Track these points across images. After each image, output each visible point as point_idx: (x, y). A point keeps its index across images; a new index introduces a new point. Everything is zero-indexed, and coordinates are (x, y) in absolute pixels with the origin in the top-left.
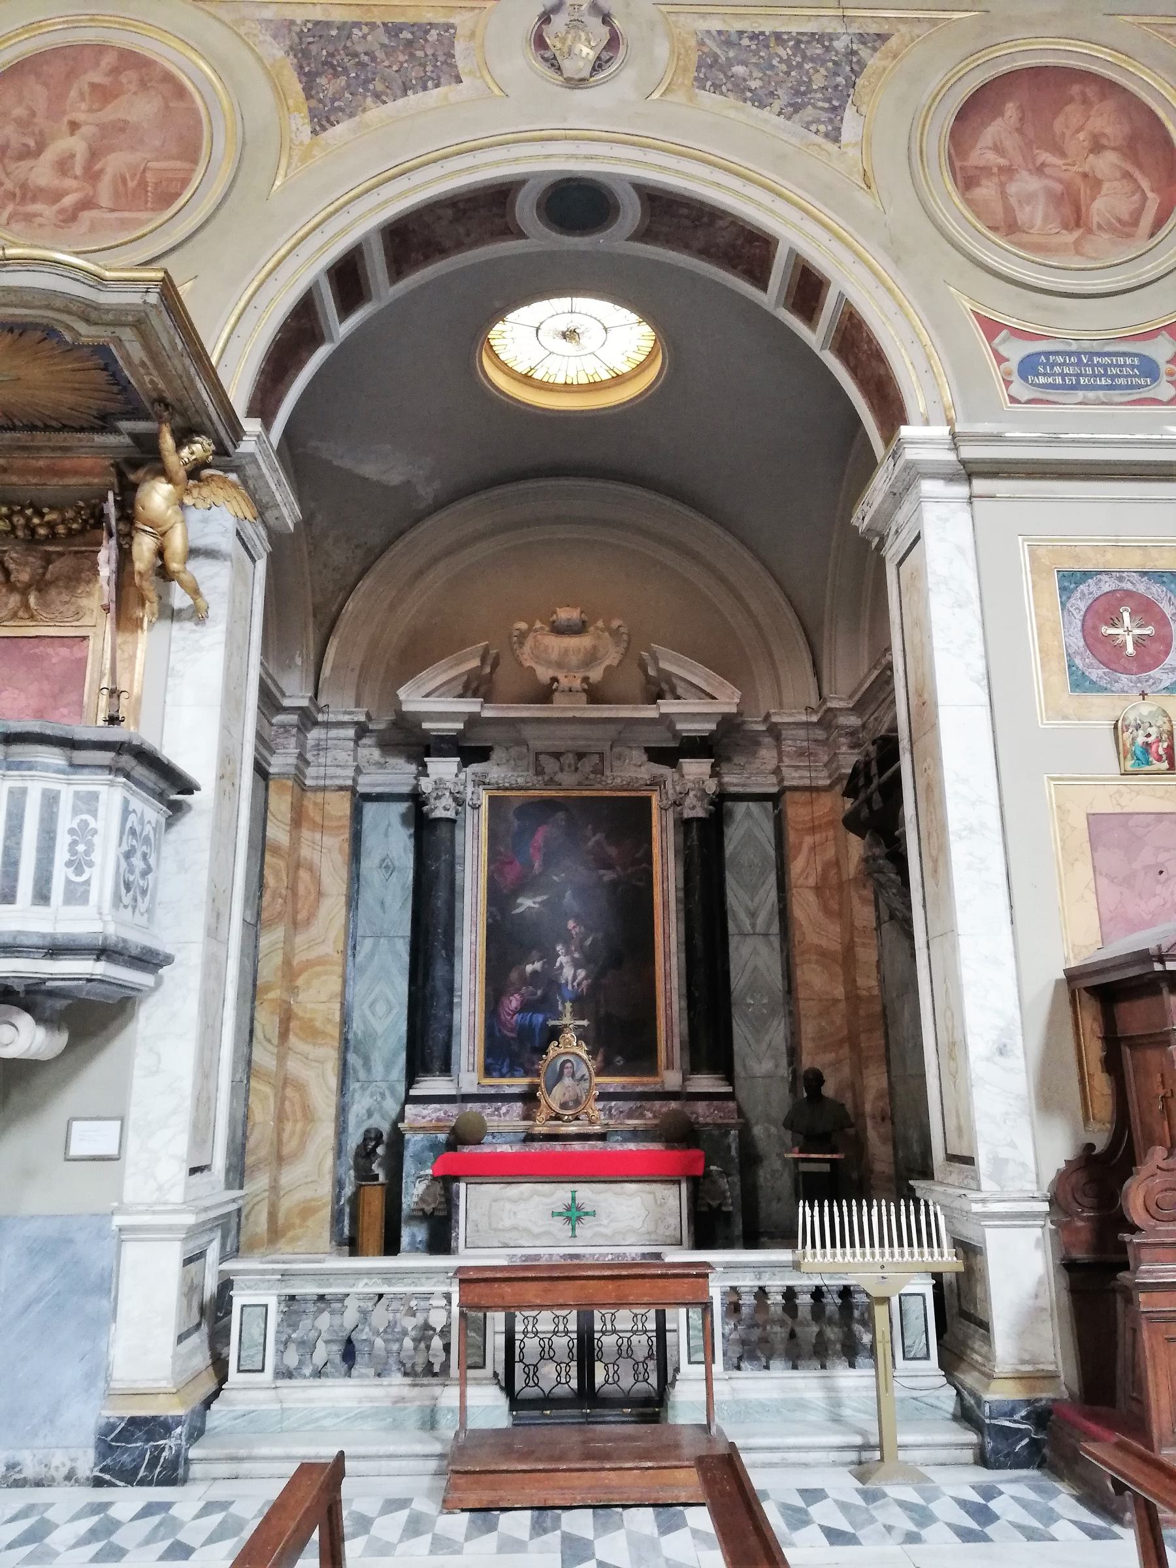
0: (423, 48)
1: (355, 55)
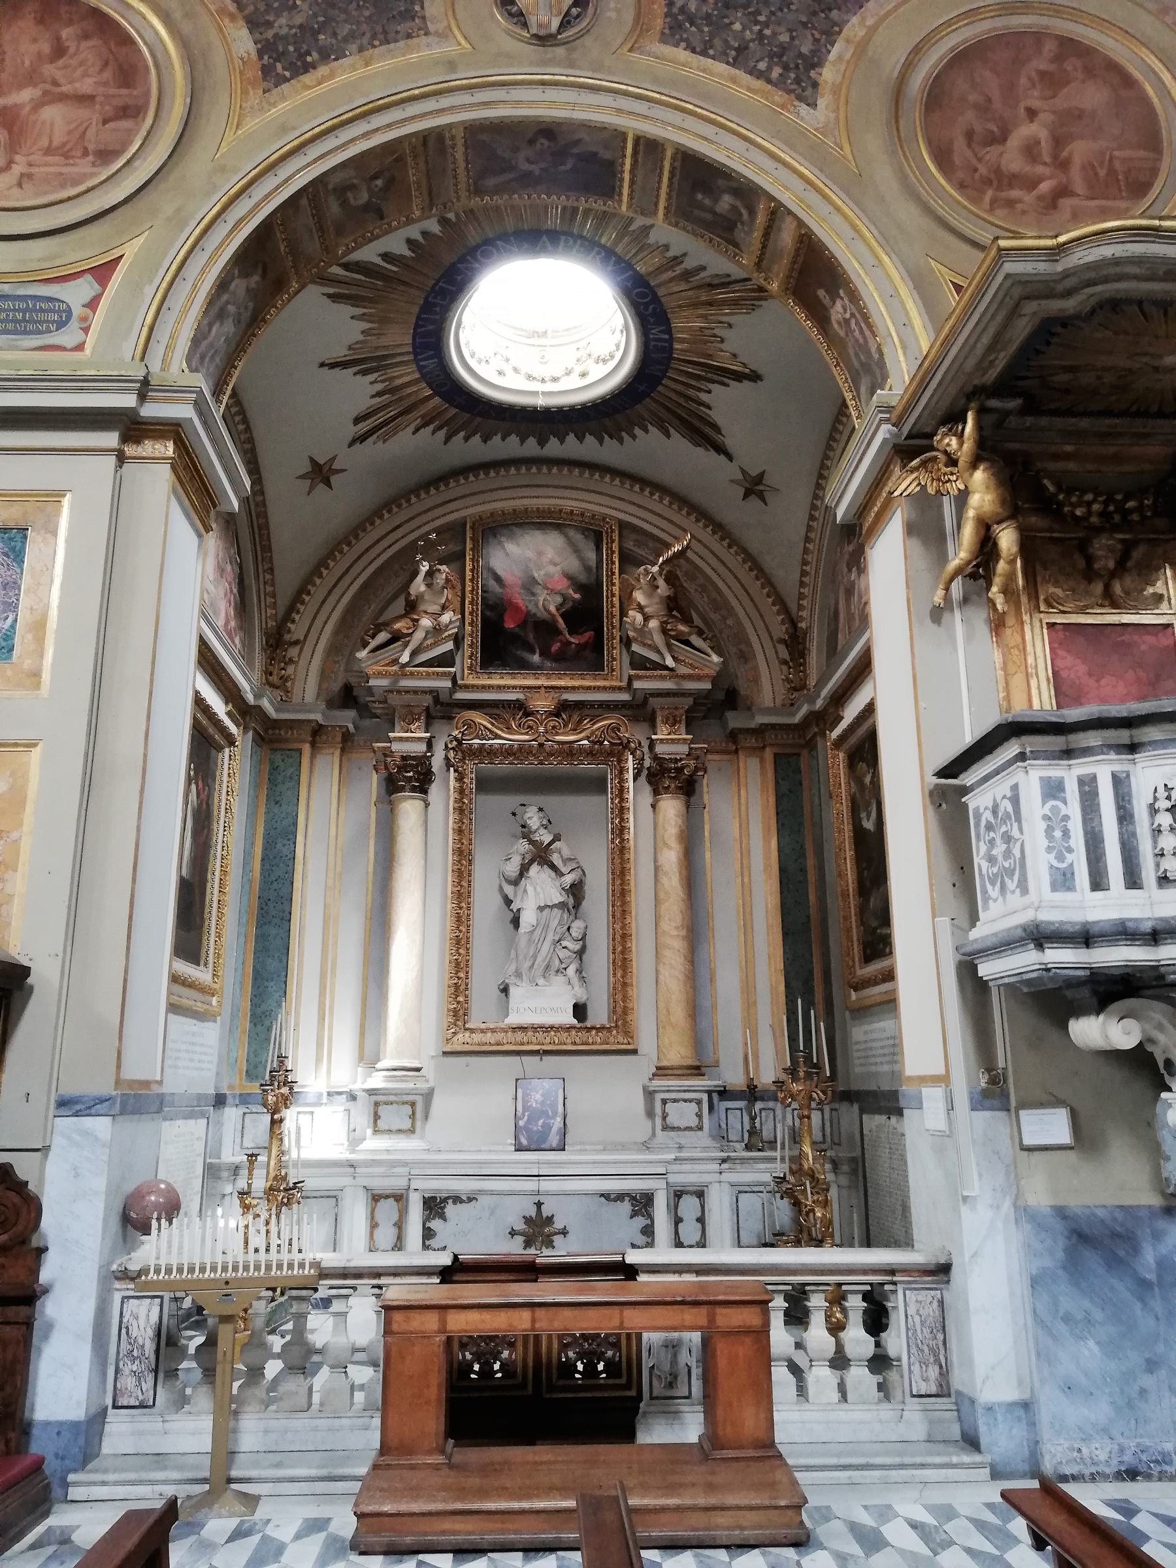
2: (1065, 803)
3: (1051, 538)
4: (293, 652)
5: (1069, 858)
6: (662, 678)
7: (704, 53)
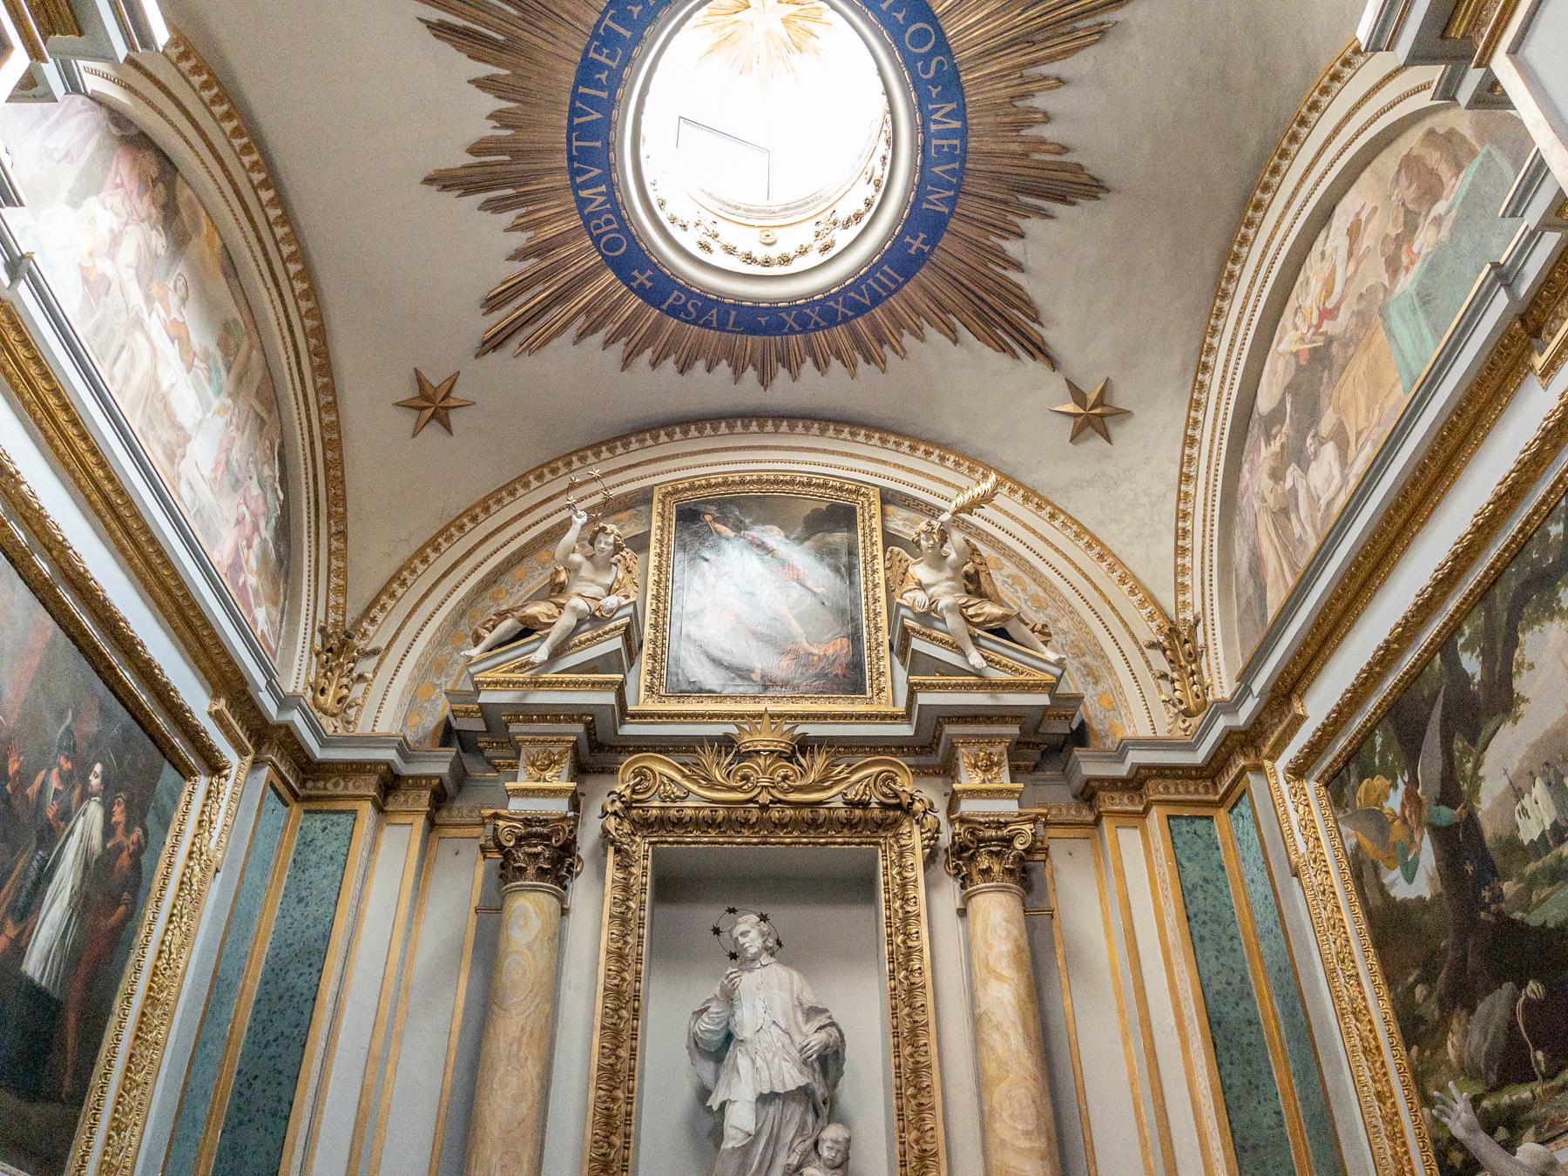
4: (366, 667)
6: (967, 687)
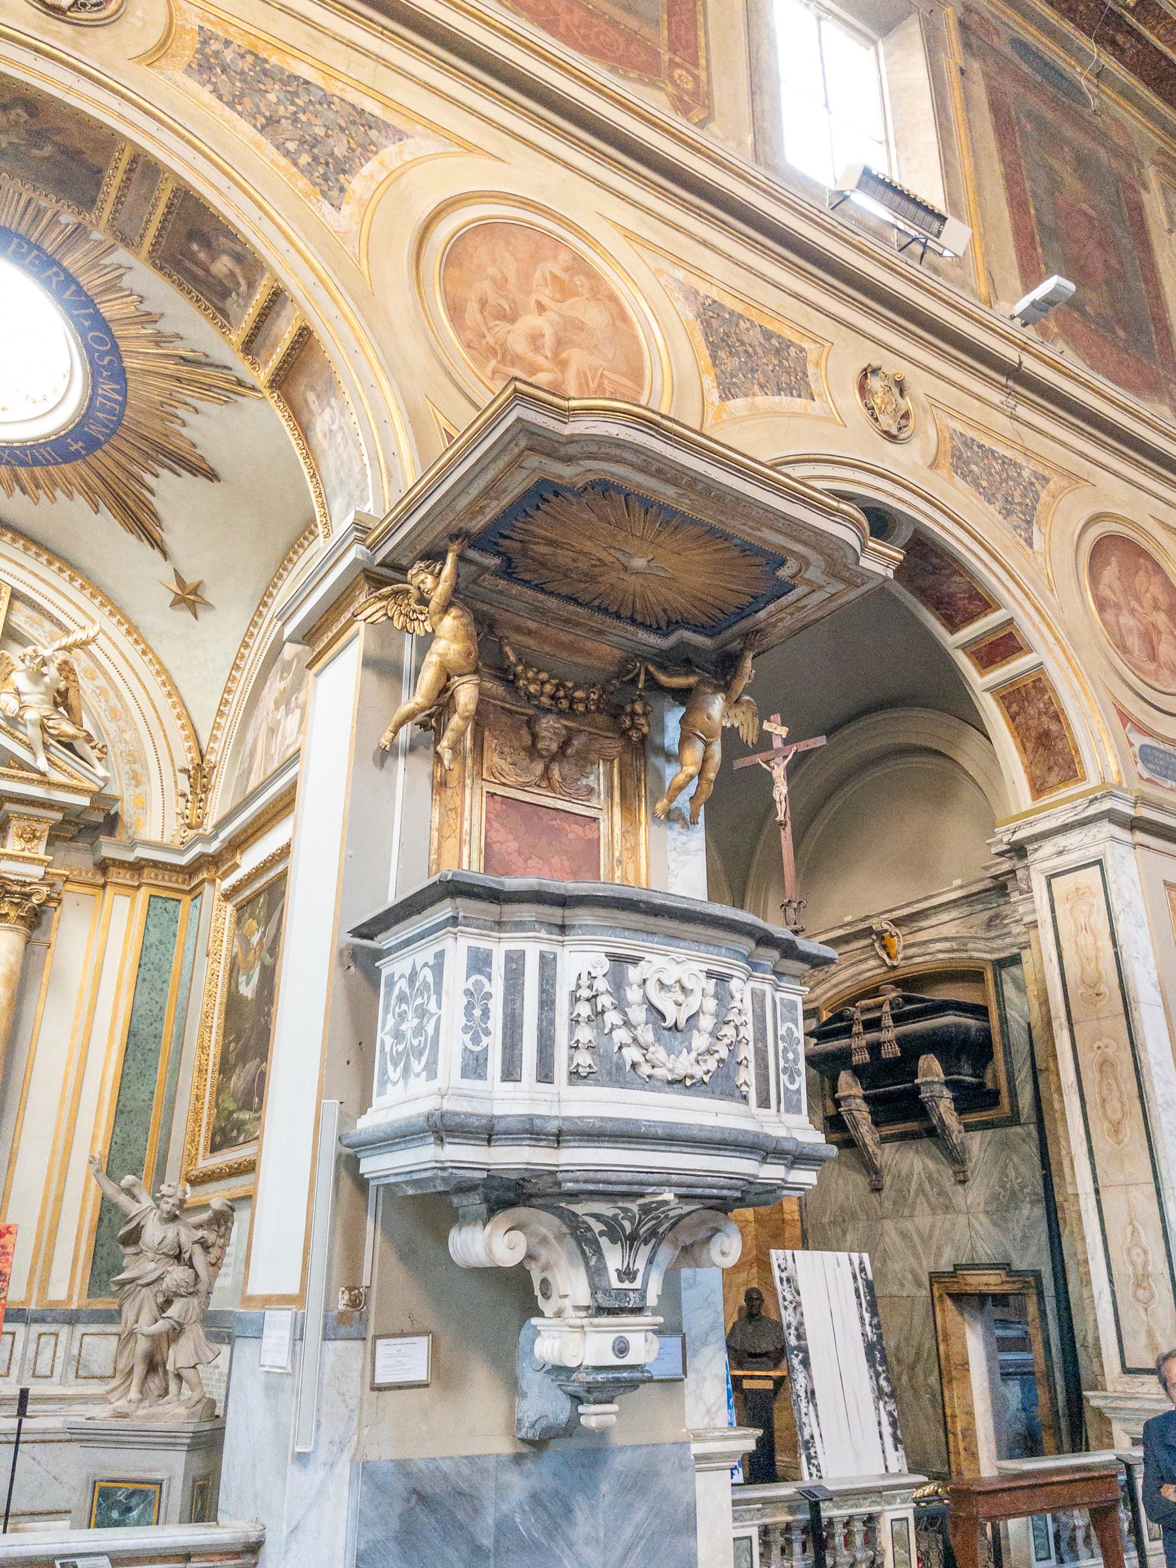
0: (787, 360)
1: (742, 343)
2: (490, 980)
3: (502, 708)
5: (485, 1040)
6: (30, 781)
7: (231, 105)
